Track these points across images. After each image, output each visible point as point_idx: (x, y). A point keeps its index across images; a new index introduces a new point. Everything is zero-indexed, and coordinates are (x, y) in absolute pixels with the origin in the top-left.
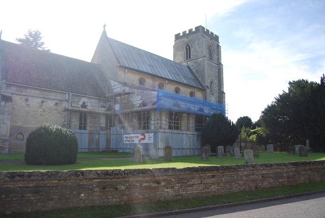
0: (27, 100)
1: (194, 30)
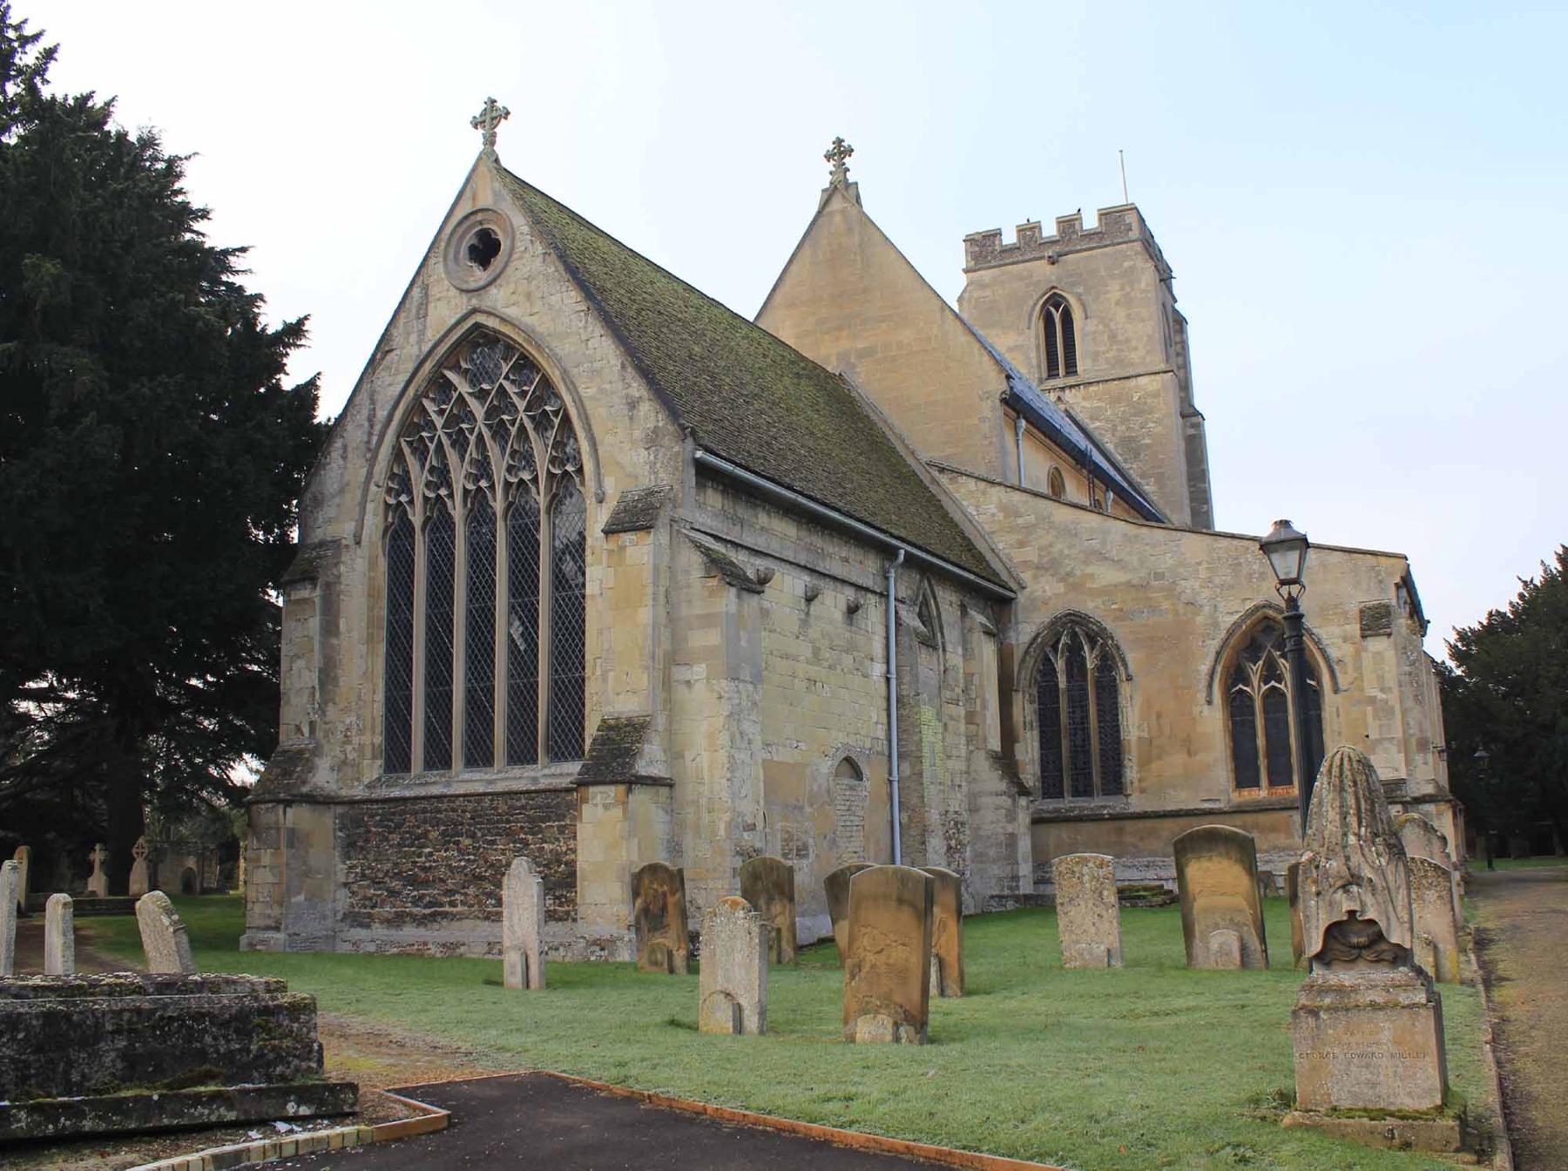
1: (1090, 222)
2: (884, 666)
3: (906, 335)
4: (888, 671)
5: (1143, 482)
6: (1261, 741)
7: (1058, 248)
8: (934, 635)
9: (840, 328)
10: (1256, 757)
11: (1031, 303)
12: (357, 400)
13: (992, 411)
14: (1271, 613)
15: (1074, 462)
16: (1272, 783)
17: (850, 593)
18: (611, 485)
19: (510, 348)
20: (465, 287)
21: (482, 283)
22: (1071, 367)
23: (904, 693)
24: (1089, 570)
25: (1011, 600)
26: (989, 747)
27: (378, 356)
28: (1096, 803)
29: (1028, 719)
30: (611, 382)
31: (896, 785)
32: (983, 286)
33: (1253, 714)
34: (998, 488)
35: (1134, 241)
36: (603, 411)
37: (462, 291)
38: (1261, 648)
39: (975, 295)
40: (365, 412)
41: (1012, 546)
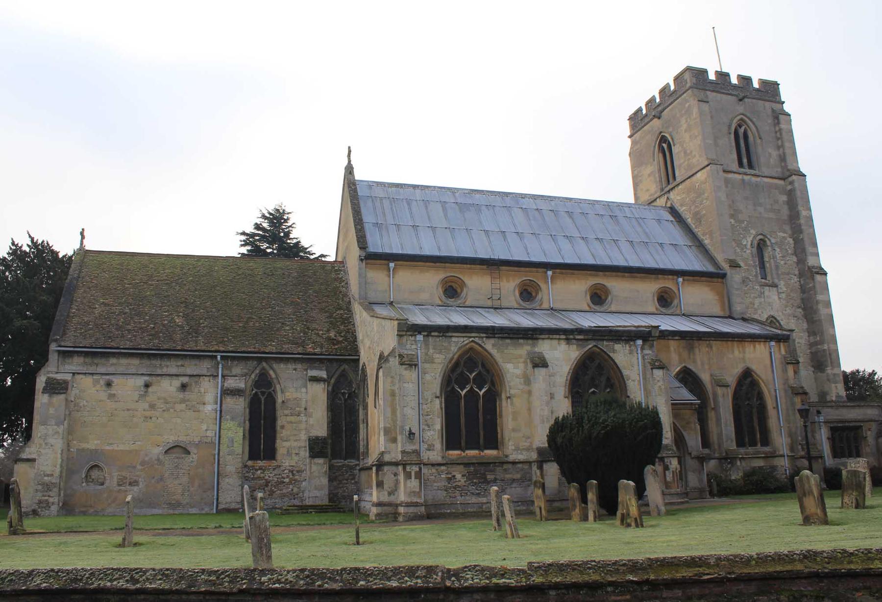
0: (109, 384)
15: (485, 267)
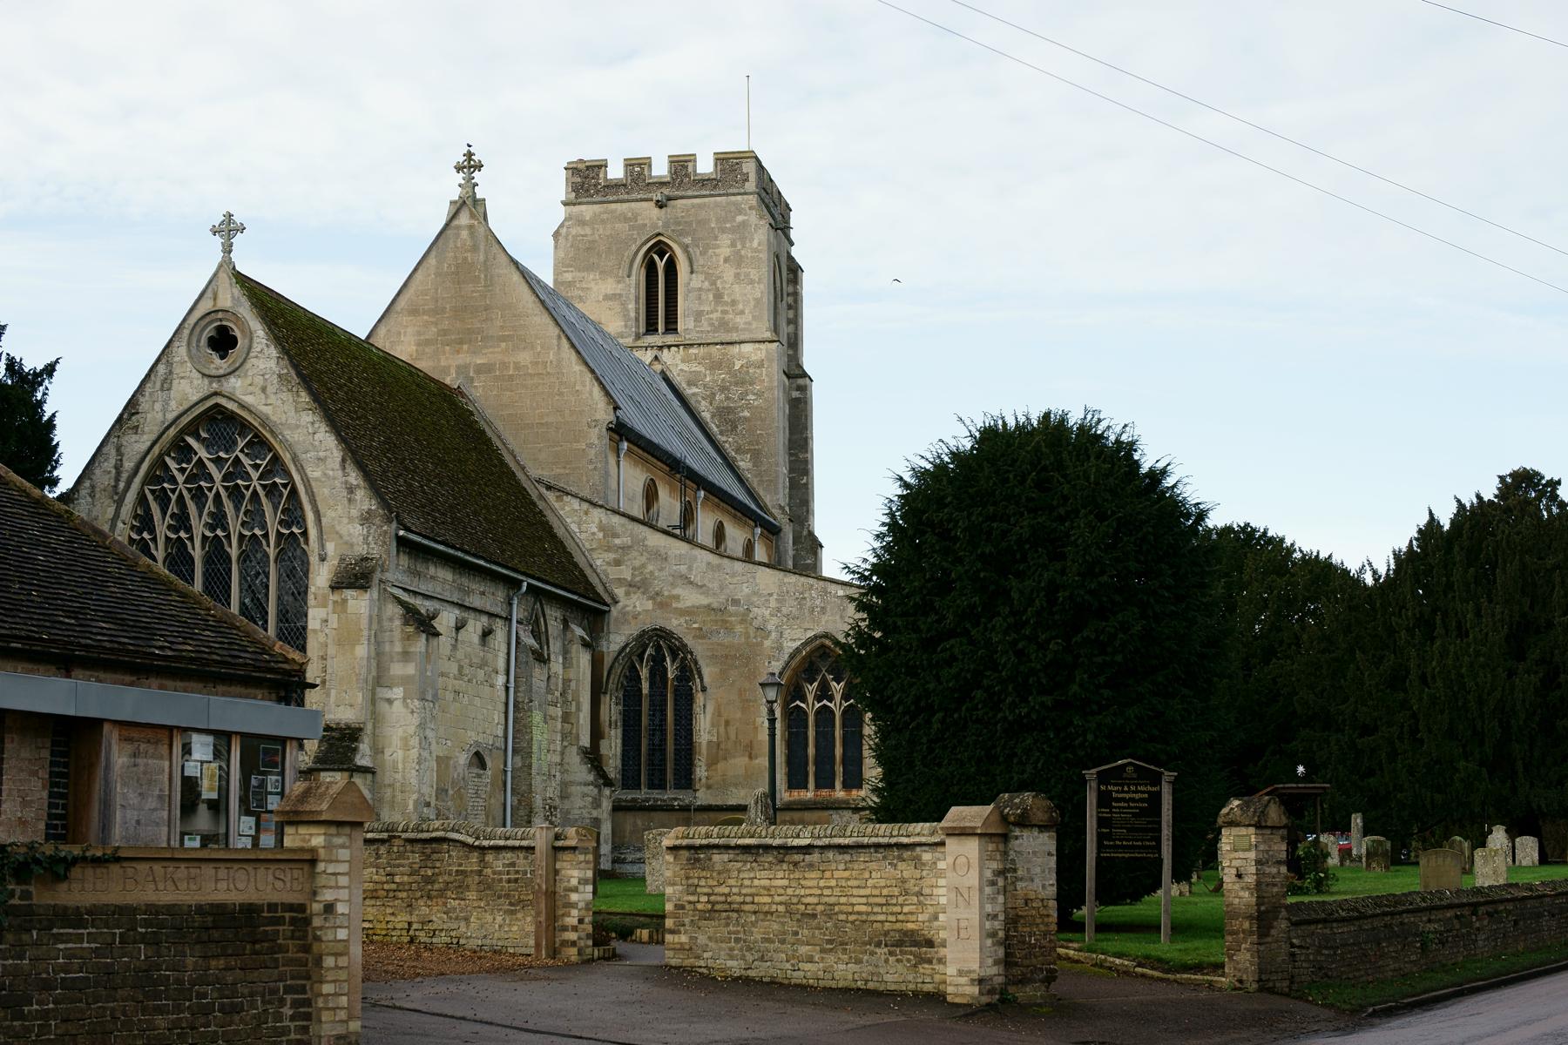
1: (705, 166)
2: (505, 677)
3: (524, 357)
4: (508, 681)
5: (738, 458)
6: (811, 751)
7: (666, 191)
8: (541, 648)
9: (461, 342)
10: (807, 764)
11: (634, 248)
12: (105, 450)
13: (597, 437)
14: (828, 642)
15: (668, 469)
16: (818, 787)
17: (484, 619)
18: (330, 547)
19: (244, 426)
20: (207, 373)
21: (221, 372)
22: (671, 326)
23: (520, 700)
24: (676, 592)
25: (604, 612)
26: (581, 744)
27: (125, 416)
28: (668, 795)
29: (613, 718)
30: (333, 470)
31: (509, 774)
32: (581, 222)
33: (806, 727)
34: (599, 510)
35: (751, 193)
36: (326, 491)
37: (204, 375)
38: (818, 671)
39: (574, 231)
40: (113, 462)
41: (608, 564)
